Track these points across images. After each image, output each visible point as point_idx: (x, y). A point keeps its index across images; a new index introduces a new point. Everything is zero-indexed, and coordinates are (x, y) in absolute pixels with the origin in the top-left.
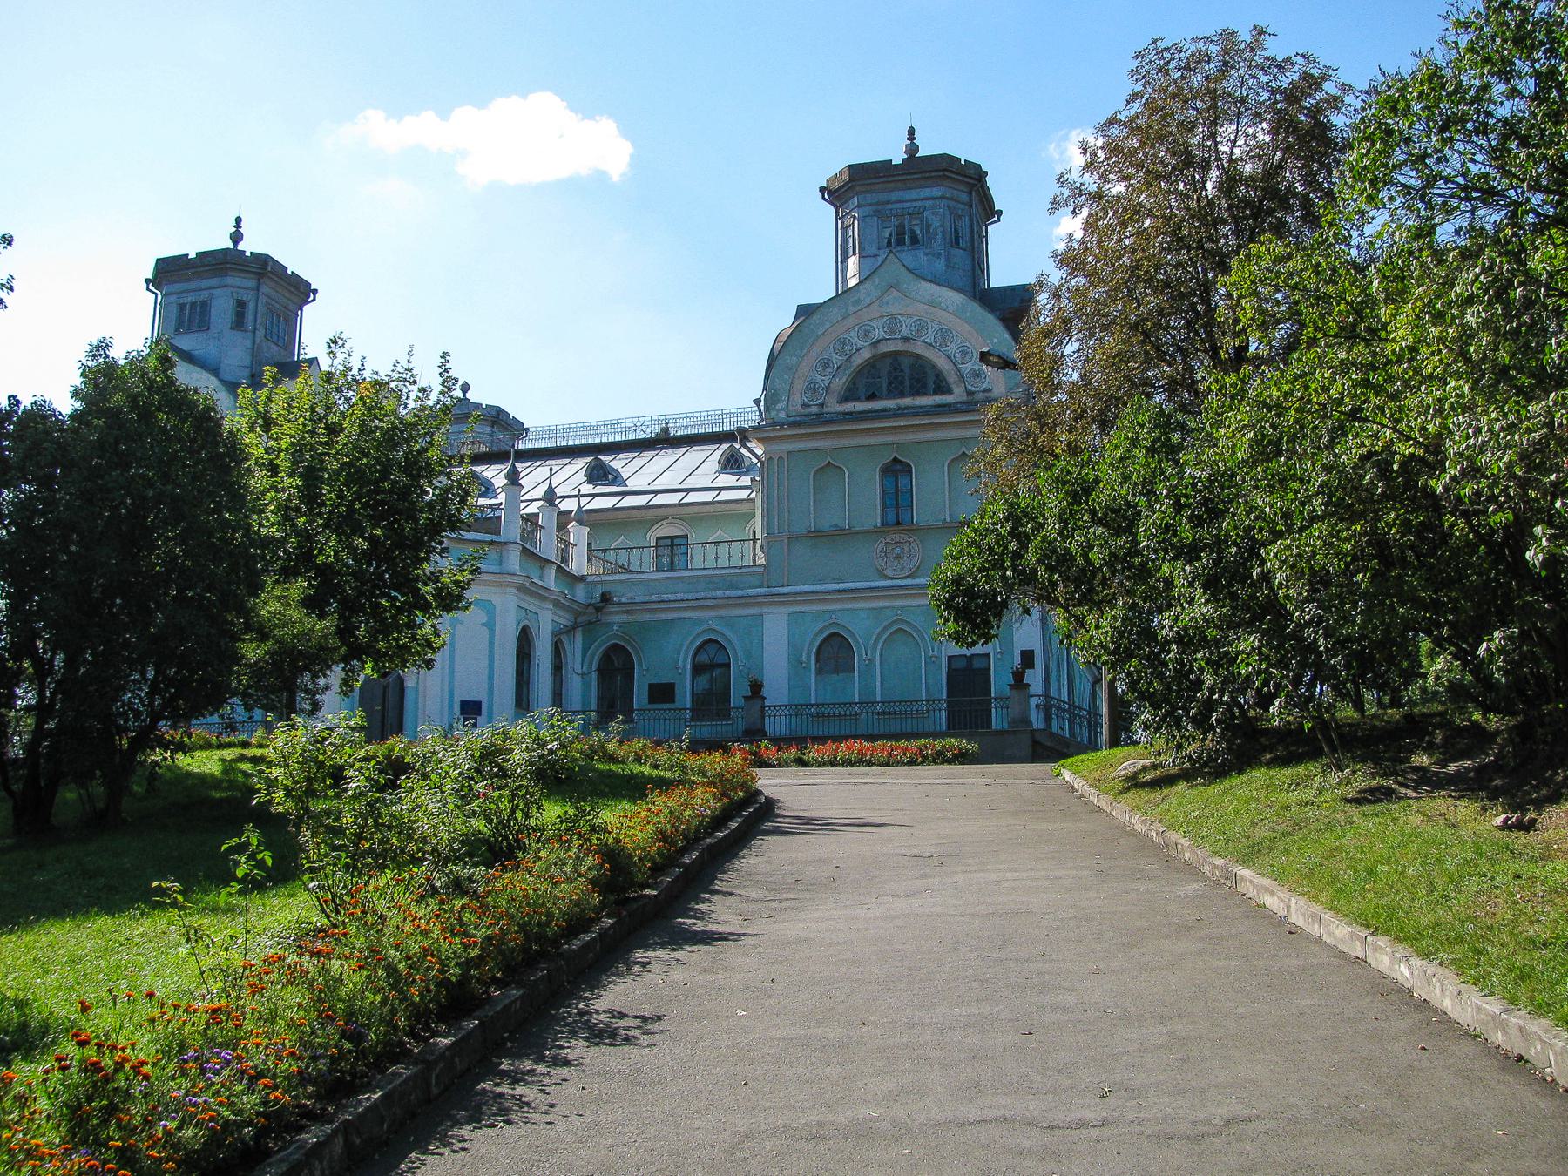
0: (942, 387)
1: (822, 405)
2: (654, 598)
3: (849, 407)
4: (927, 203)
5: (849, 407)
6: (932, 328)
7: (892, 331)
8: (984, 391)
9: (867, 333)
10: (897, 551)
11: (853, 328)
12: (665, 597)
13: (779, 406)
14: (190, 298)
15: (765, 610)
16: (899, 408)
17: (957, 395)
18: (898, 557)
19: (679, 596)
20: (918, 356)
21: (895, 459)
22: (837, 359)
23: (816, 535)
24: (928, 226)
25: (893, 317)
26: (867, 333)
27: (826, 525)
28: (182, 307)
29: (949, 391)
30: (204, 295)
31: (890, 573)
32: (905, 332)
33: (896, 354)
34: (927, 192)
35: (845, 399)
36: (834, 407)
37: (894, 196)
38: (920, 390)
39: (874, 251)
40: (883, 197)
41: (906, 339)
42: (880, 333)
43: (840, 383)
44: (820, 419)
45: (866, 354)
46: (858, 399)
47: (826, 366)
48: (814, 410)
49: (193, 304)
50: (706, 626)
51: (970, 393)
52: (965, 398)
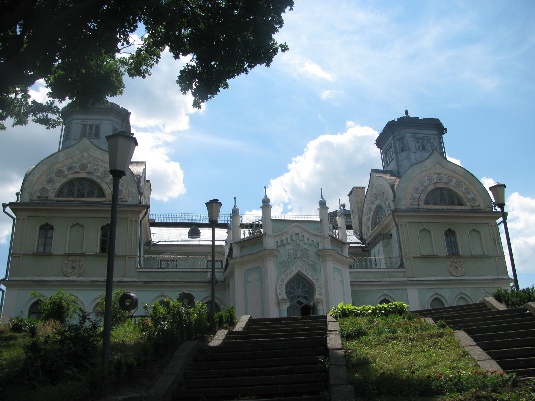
0: (460, 203)
1: (418, 205)
2: (358, 280)
3: (429, 207)
4: (432, 136)
5: (429, 207)
6: (455, 180)
7: (440, 179)
8: (477, 206)
9: (430, 180)
10: (456, 265)
11: (425, 176)
12: (364, 280)
13: (402, 203)
14: (90, 123)
15: (407, 287)
16: (448, 209)
17: (468, 207)
18: (457, 268)
19: (370, 280)
20: (450, 190)
21: (449, 229)
22: (421, 188)
23: (423, 257)
24: (433, 144)
25: (439, 174)
26: (430, 180)
27: (425, 253)
28: (85, 126)
29: (461, 204)
30: (97, 123)
31: (454, 274)
32: (444, 181)
33: (441, 189)
34: (430, 132)
35: (427, 203)
36: (423, 206)
37: (419, 131)
38: (452, 203)
39: (415, 150)
40: (416, 131)
41: (446, 183)
42: (435, 180)
43: (423, 197)
44: (418, 210)
45: (431, 187)
46: (429, 204)
47: (417, 190)
48: (415, 206)
49: (91, 126)
50: (382, 293)
51: (473, 206)
52: (471, 208)
